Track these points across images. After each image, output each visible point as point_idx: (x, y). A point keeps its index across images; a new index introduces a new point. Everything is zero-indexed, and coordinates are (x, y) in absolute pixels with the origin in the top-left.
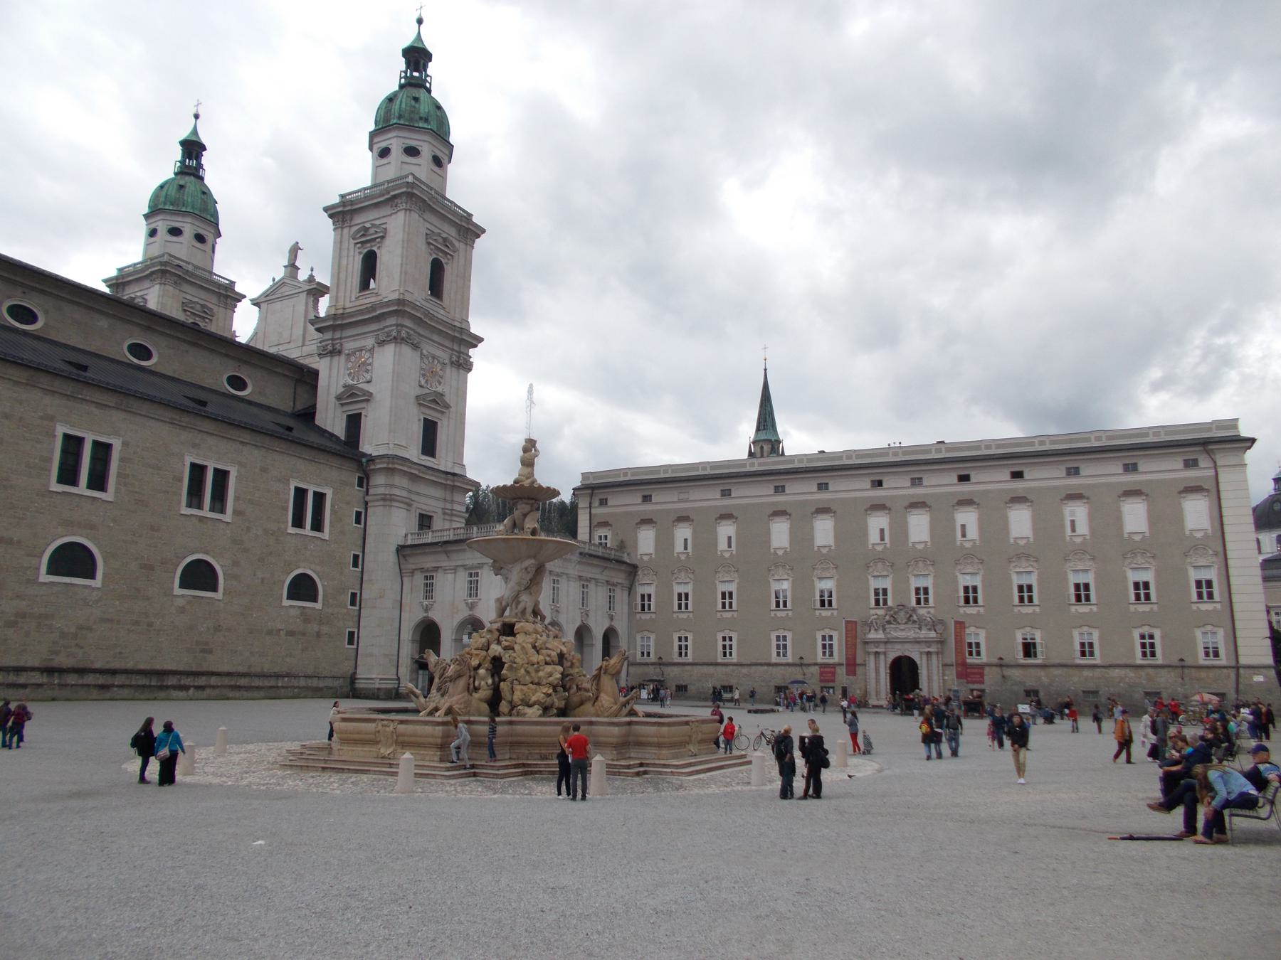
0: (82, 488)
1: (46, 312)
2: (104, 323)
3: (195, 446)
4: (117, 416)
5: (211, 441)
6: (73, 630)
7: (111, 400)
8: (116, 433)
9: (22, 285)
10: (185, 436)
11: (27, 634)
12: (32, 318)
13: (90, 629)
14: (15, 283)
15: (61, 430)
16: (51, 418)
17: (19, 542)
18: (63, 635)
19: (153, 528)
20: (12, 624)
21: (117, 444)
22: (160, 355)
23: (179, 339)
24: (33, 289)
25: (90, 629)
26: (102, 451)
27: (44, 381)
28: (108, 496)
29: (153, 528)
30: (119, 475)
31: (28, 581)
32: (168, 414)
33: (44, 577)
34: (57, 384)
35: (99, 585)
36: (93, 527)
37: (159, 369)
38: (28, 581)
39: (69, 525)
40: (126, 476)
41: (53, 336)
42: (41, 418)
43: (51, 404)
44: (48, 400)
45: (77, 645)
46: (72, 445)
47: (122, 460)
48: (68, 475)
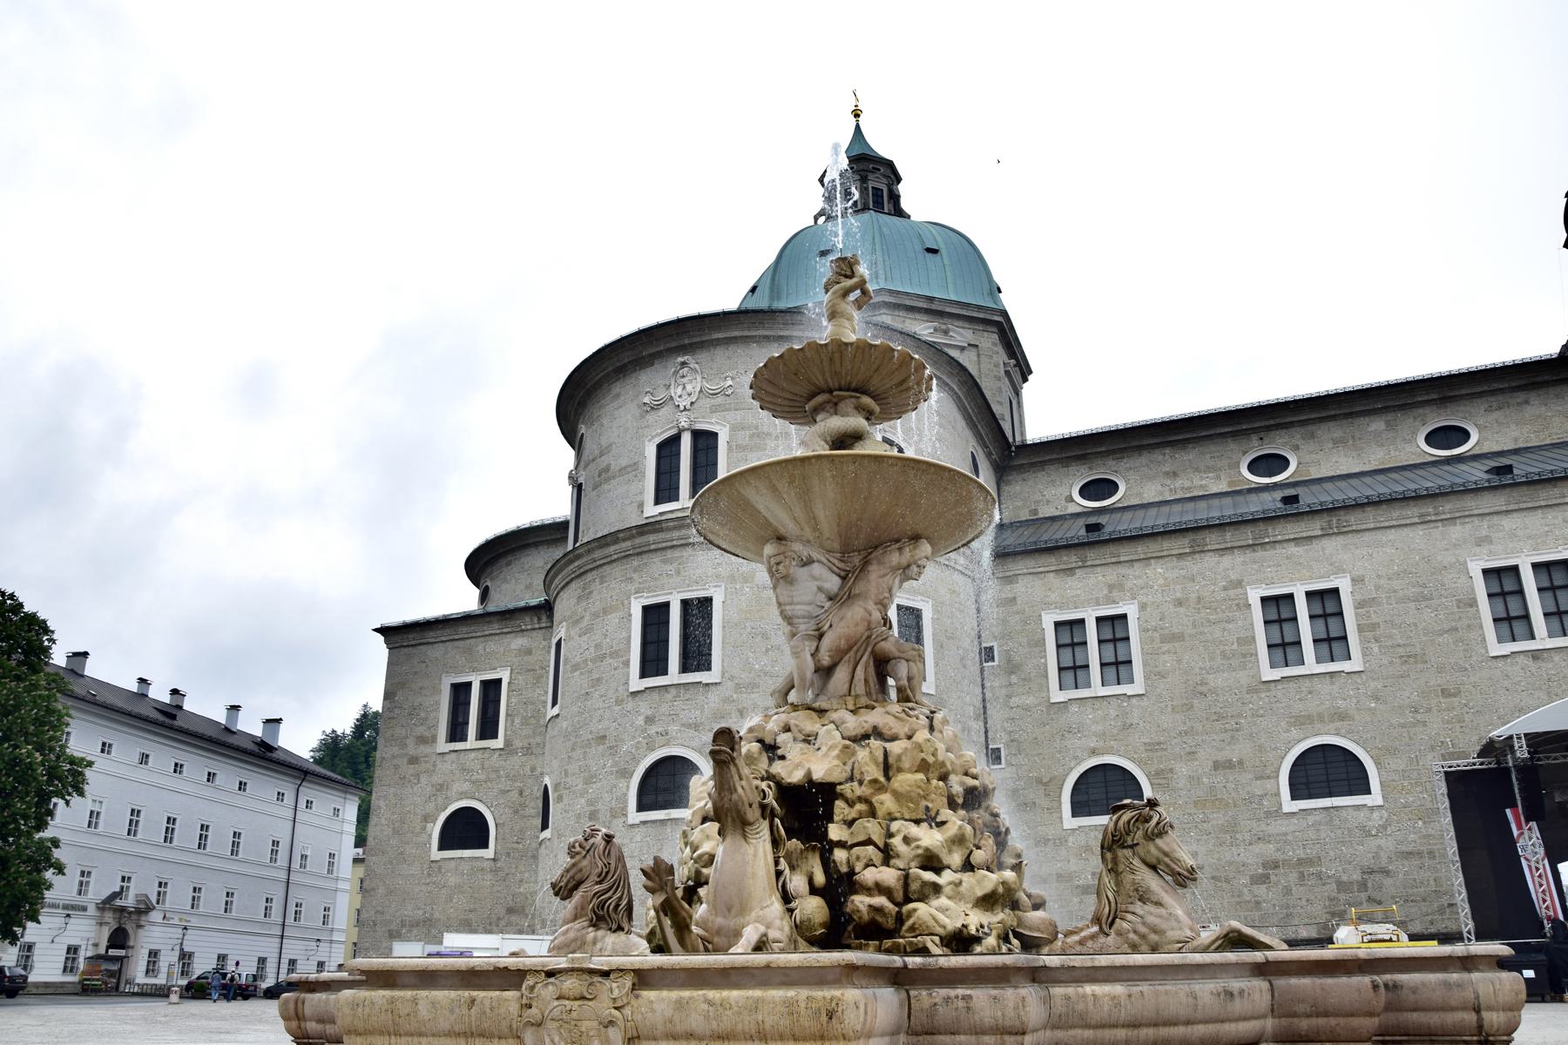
0: (1311, 665)
1: (1296, 448)
2: (1377, 425)
3: (1480, 542)
4: (1330, 545)
5: (1508, 523)
6: (1356, 876)
7: (1314, 527)
8: (1339, 570)
9: (1255, 430)
10: (1456, 531)
11: (1287, 891)
12: (1283, 463)
13: (1387, 873)
14: (1246, 433)
15: (1254, 596)
16: (1239, 584)
17: (1241, 762)
18: (1342, 886)
19: (1445, 693)
20: (1263, 879)
21: (1344, 585)
22: (1480, 428)
23: (1502, 391)
24: (1269, 428)
25: (1387, 873)
26: (1325, 601)
27: (1212, 540)
28: (1355, 664)
29: (1445, 693)
30: (1360, 629)
31: (1268, 814)
32: (1412, 512)
33: (1289, 805)
34: (1229, 536)
35: (1380, 802)
36: (1342, 716)
37: (1486, 449)
38: (1268, 814)
39: (1304, 722)
40: (1374, 626)
41: (1315, 474)
42: (1225, 589)
43: (1233, 565)
44: (1226, 560)
45: (1370, 899)
46: (1277, 606)
47: (1359, 605)
48: (1284, 649)
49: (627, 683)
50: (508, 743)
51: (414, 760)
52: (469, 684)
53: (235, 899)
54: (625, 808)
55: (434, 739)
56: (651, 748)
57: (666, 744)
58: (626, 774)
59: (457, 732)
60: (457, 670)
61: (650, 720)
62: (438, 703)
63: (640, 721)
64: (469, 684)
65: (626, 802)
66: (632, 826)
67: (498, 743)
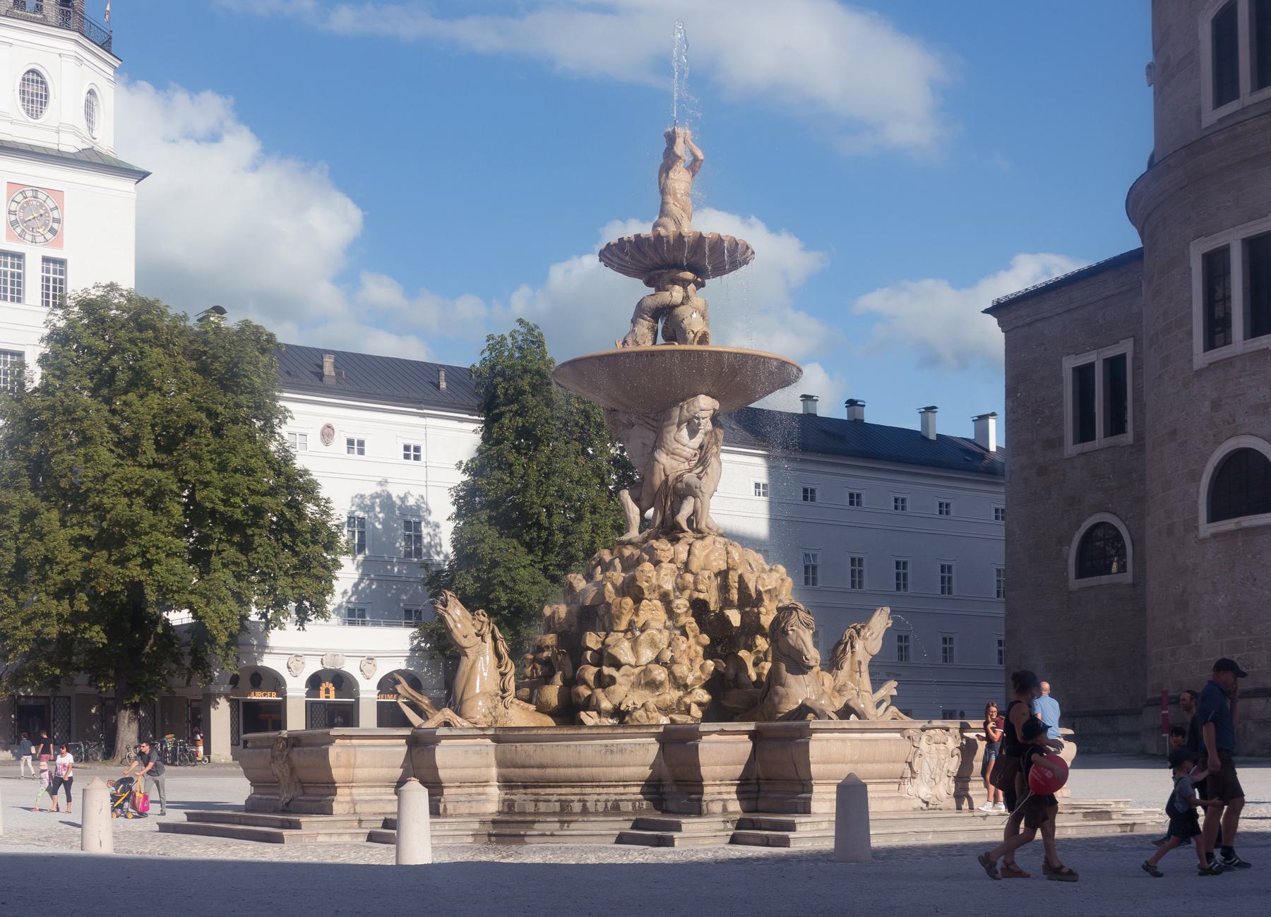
49: (1191, 360)
50: (1139, 437)
51: (1042, 471)
52: (1091, 366)
53: (955, 645)
54: (1196, 519)
55: (1061, 441)
56: (1219, 443)
57: (1234, 435)
58: (1195, 477)
59: (1085, 431)
60: (1078, 352)
61: (1216, 405)
62: (1061, 395)
63: (1206, 407)
64: (1091, 366)
65: (1196, 511)
66: (1204, 541)
67: (1128, 438)
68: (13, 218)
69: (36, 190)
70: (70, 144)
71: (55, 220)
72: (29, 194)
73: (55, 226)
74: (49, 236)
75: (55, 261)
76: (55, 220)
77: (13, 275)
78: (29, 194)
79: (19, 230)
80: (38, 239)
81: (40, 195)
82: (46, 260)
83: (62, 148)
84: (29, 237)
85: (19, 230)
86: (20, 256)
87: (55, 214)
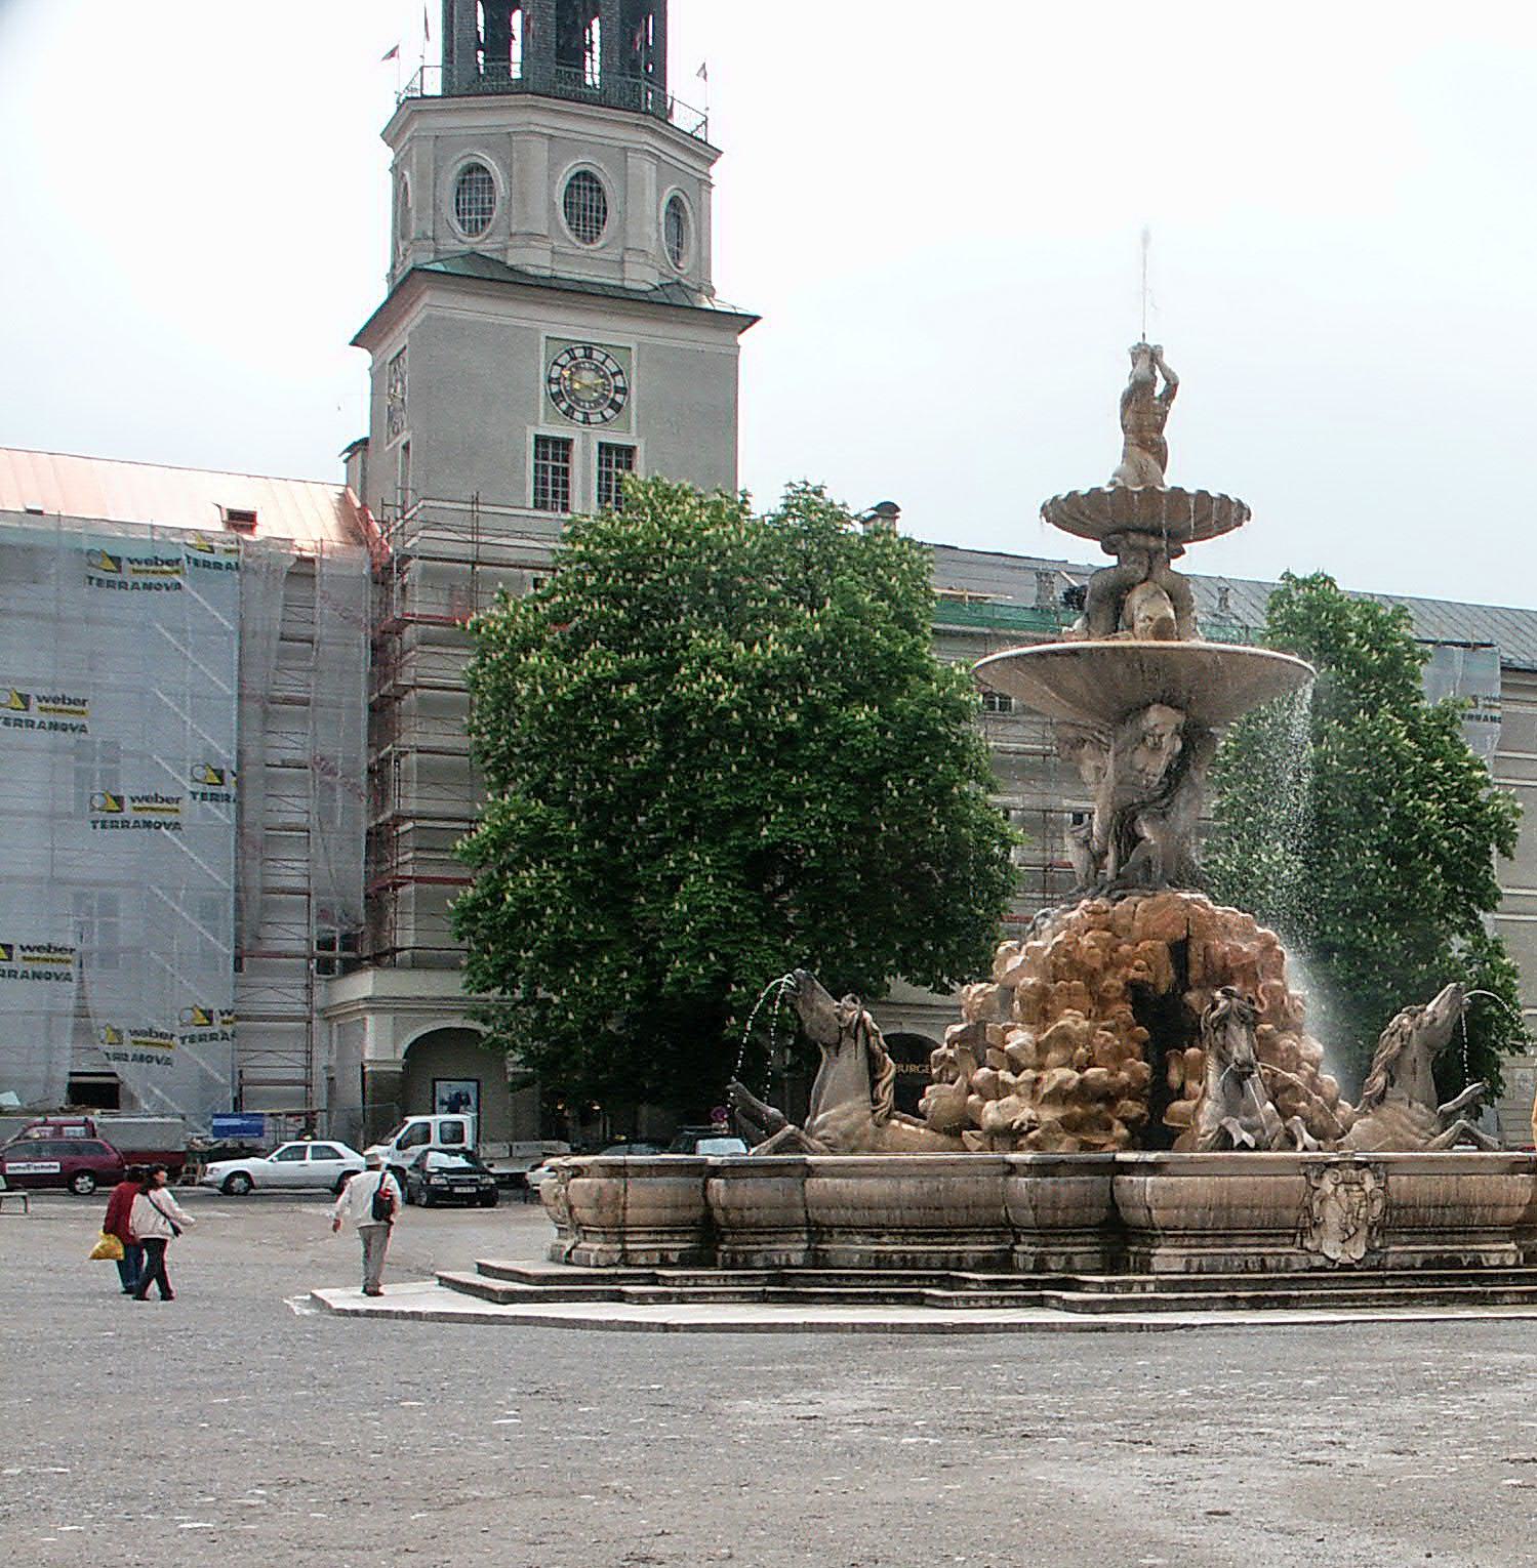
68: (555, 388)
69: (588, 350)
70: (642, 277)
71: (618, 390)
72: (579, 353)
73: (619, 398)
74: (609, 413)
75: (619, 449)
76: (618, 390)
77: (555, 469)
78: (579, 353)
79: (564, 406)
80: (592, 419)
81: (595, 354)
82: (604, 448)
83: (627, 284)
84: (579, 416)
85: (564, 406)
86: (567, 444)
87: (619, 381)
